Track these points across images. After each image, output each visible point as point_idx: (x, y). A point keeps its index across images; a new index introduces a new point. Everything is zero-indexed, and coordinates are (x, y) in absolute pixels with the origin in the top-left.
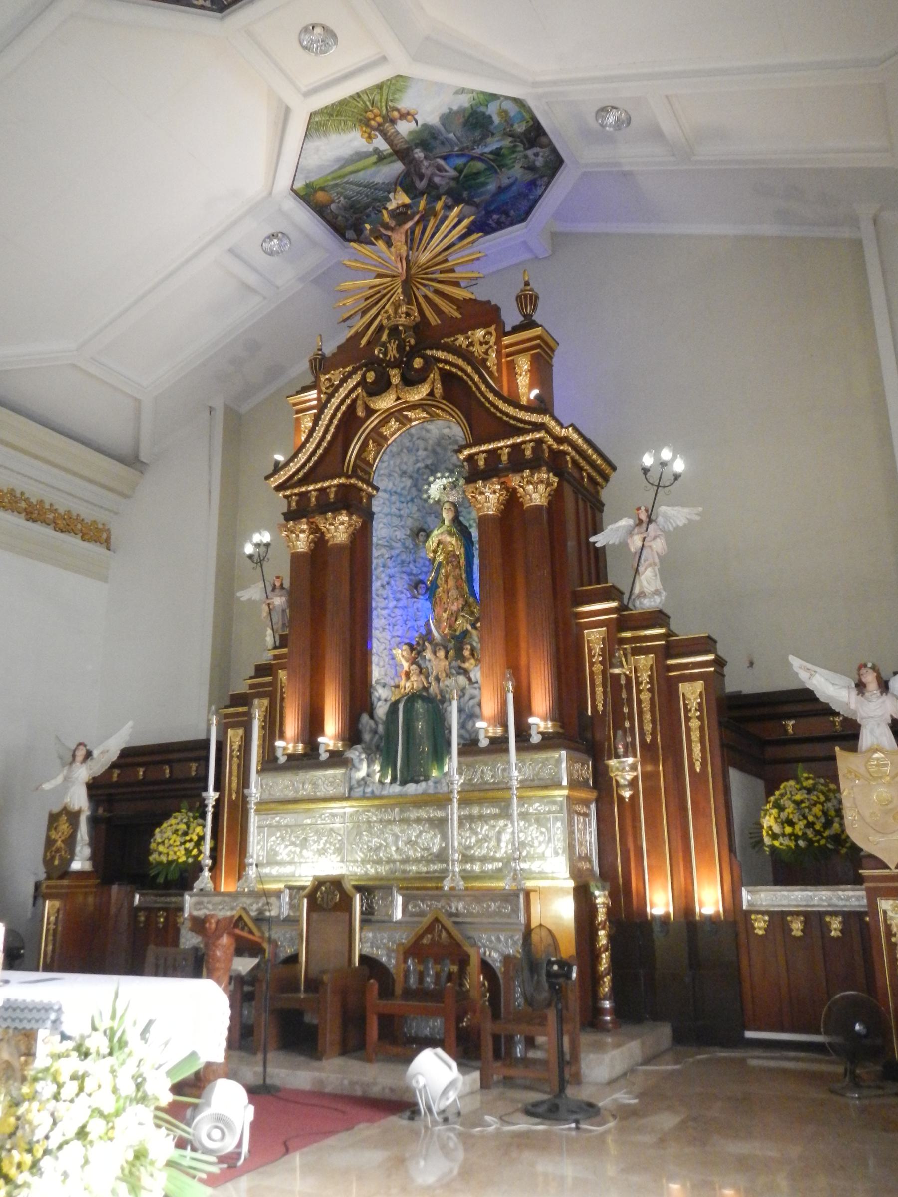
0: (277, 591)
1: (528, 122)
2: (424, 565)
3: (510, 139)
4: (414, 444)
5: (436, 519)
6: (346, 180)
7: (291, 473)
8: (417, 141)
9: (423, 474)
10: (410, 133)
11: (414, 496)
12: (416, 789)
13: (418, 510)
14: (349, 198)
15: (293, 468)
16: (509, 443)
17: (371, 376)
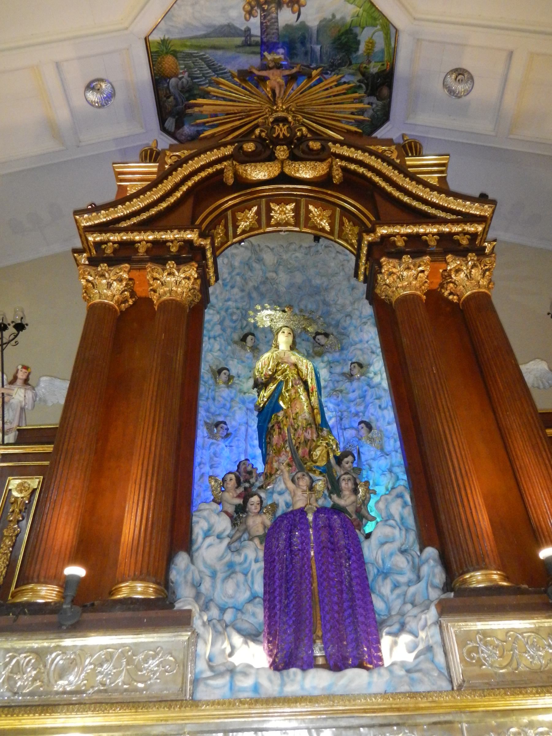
0: (19, 382)
1: (383, 65)
2: (224, 406)
3: (360, 77)
4: (232, 278)
5: (239, 365)
6: (202, 53)
7: (116, 216)
8: (287, 40)
9: (232, 314)
10: (287, 26)
11: (217, 334)
12: (369, 684)
13: (219, 350)
14: (193, 78)
15: (121, 211)
16: (435, 230)
17: (250, 147)
